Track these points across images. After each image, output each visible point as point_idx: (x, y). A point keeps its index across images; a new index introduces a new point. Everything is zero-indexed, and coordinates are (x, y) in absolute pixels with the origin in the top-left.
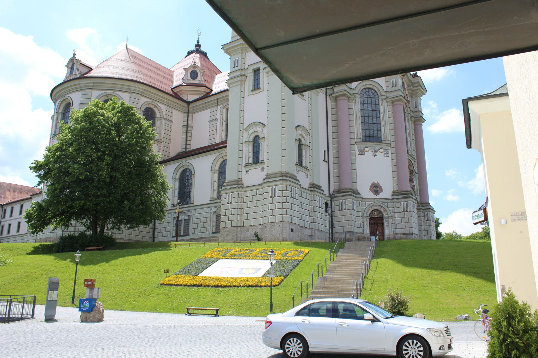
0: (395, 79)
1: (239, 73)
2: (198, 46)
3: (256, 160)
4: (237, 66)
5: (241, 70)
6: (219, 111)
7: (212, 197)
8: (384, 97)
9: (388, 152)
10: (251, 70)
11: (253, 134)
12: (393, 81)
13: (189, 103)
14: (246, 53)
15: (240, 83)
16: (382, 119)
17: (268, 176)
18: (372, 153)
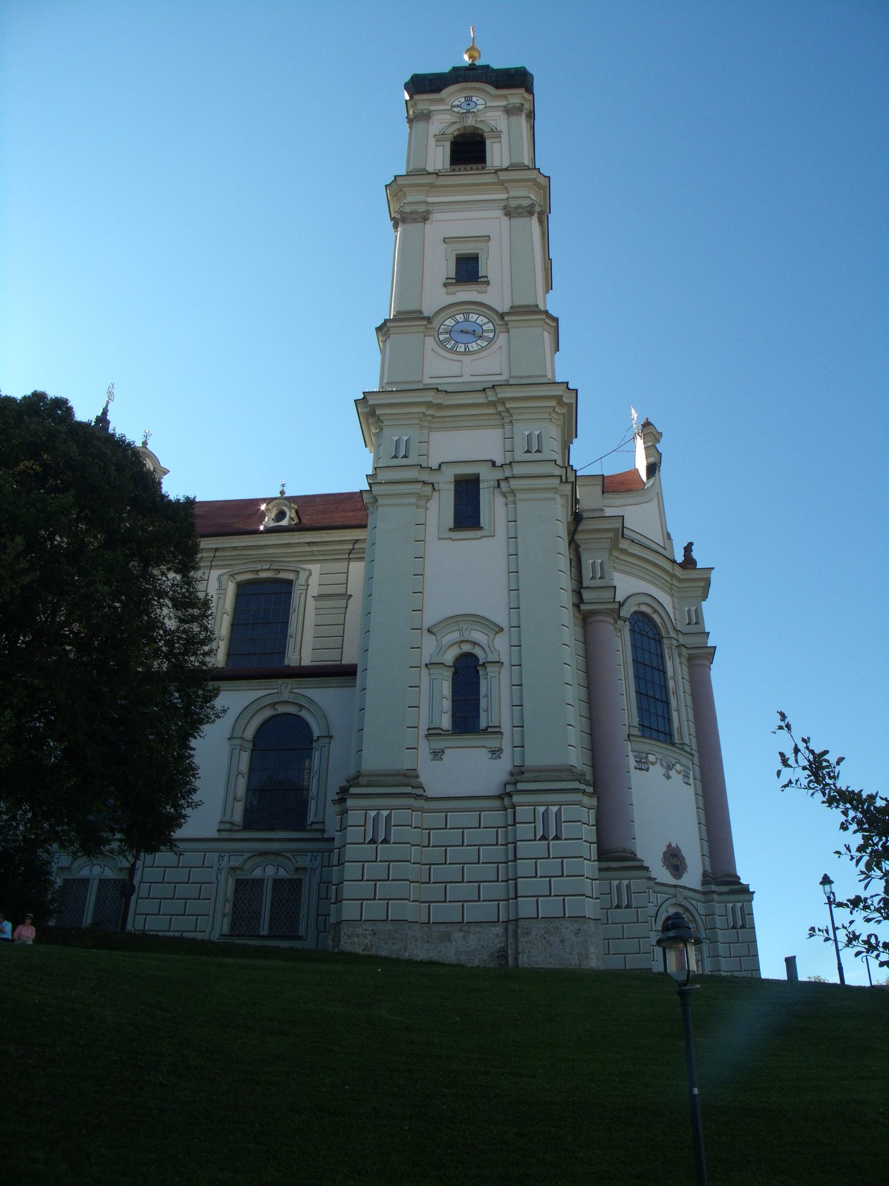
0: (694, 608)
4: (405, 456)
5: (418, 468)
7: (227, 818)
8: (675, 643)
9: (689, 774)
11: (455, 647)
12: (689, 612)
16: (673, 693)
17: (518, 773)
18: (663, 771)
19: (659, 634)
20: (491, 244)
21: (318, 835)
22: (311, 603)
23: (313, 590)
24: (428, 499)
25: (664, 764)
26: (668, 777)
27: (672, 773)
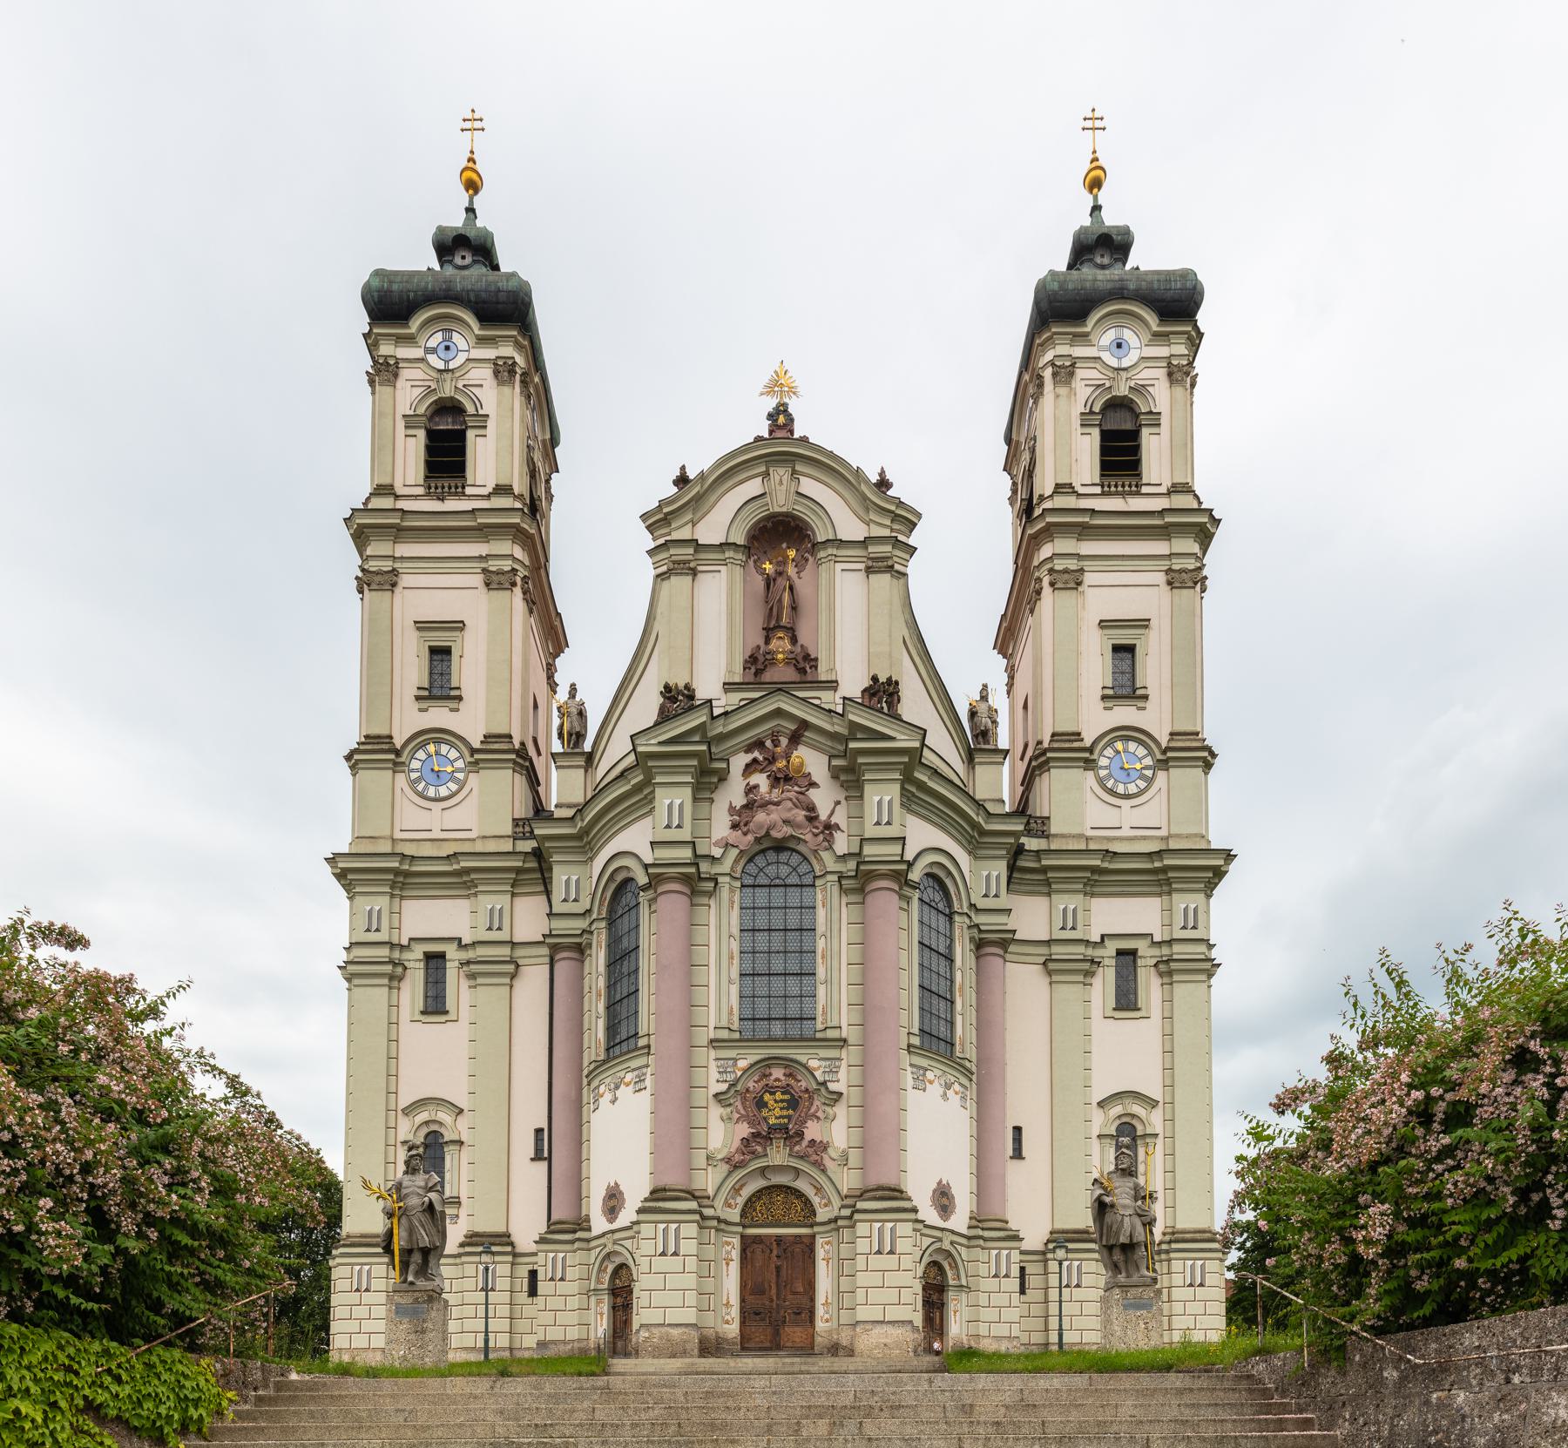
1: (384, 952)
10: (418, 952)
14: (402, 898)
15: (386, 981)
20: (467, 633)
24: (401, 979)
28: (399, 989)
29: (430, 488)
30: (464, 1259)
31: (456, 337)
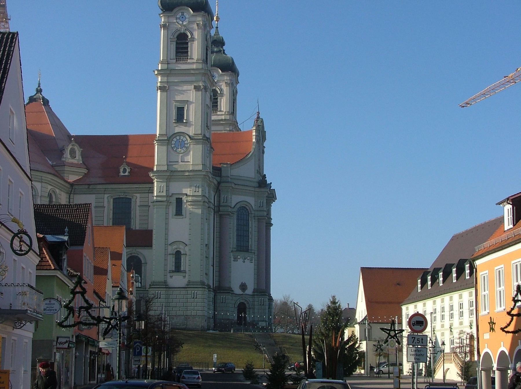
2: (39, 91)
3: (178, 269)
4: (162, 192)
6: (106, 200)
12: (260, 202)
13: (72, 185)
14: (169, 182)
16: (251, 233)
17: (189, 282)
19: (248, 212)
21: (144, 289)
22: (137, 207)
23: (138, 204)
25: (243, 258)
26: (244, 262)
27: (246, 261)
28: (169, 208)
29: (177, 59)
30: (188, 289)
31: (185, 14)
